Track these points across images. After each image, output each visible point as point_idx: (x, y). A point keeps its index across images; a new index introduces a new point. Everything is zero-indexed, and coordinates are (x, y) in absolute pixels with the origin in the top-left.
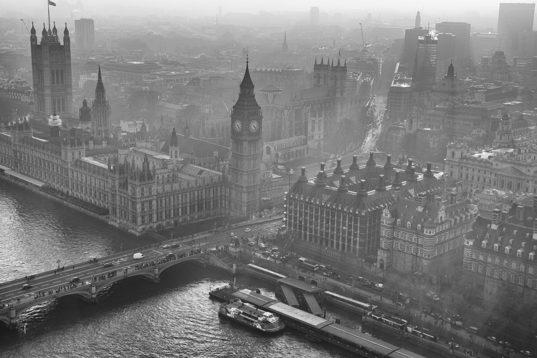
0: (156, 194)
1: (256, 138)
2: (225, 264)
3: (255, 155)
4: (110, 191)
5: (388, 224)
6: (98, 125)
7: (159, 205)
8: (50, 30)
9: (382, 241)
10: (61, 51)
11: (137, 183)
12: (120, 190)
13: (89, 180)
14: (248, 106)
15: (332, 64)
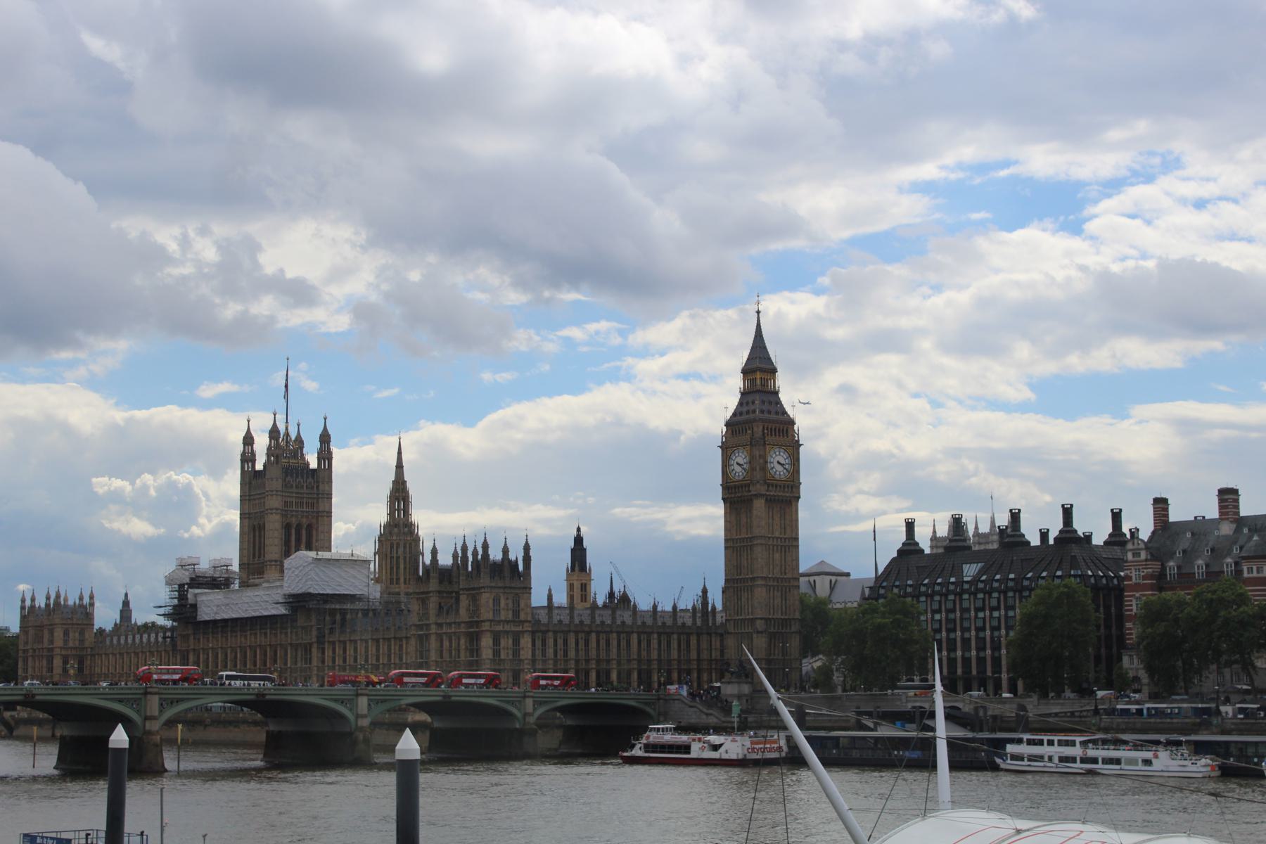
0: (529, 619)
1: (787, 495)
2: (711, 711)
3: (785, 539)
4: (414, 632)
5: (1145, 578)
6: (391, 583)
7: (537, 652)
8: (287, 434)
9: (1130, 629)
10: (310, 479)
11: (485, 580)
12: (439, 621)
13: (363, 650)
14: (762, 412)
15: (976, 528)
